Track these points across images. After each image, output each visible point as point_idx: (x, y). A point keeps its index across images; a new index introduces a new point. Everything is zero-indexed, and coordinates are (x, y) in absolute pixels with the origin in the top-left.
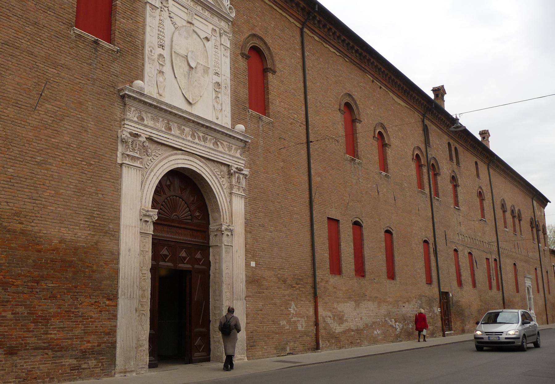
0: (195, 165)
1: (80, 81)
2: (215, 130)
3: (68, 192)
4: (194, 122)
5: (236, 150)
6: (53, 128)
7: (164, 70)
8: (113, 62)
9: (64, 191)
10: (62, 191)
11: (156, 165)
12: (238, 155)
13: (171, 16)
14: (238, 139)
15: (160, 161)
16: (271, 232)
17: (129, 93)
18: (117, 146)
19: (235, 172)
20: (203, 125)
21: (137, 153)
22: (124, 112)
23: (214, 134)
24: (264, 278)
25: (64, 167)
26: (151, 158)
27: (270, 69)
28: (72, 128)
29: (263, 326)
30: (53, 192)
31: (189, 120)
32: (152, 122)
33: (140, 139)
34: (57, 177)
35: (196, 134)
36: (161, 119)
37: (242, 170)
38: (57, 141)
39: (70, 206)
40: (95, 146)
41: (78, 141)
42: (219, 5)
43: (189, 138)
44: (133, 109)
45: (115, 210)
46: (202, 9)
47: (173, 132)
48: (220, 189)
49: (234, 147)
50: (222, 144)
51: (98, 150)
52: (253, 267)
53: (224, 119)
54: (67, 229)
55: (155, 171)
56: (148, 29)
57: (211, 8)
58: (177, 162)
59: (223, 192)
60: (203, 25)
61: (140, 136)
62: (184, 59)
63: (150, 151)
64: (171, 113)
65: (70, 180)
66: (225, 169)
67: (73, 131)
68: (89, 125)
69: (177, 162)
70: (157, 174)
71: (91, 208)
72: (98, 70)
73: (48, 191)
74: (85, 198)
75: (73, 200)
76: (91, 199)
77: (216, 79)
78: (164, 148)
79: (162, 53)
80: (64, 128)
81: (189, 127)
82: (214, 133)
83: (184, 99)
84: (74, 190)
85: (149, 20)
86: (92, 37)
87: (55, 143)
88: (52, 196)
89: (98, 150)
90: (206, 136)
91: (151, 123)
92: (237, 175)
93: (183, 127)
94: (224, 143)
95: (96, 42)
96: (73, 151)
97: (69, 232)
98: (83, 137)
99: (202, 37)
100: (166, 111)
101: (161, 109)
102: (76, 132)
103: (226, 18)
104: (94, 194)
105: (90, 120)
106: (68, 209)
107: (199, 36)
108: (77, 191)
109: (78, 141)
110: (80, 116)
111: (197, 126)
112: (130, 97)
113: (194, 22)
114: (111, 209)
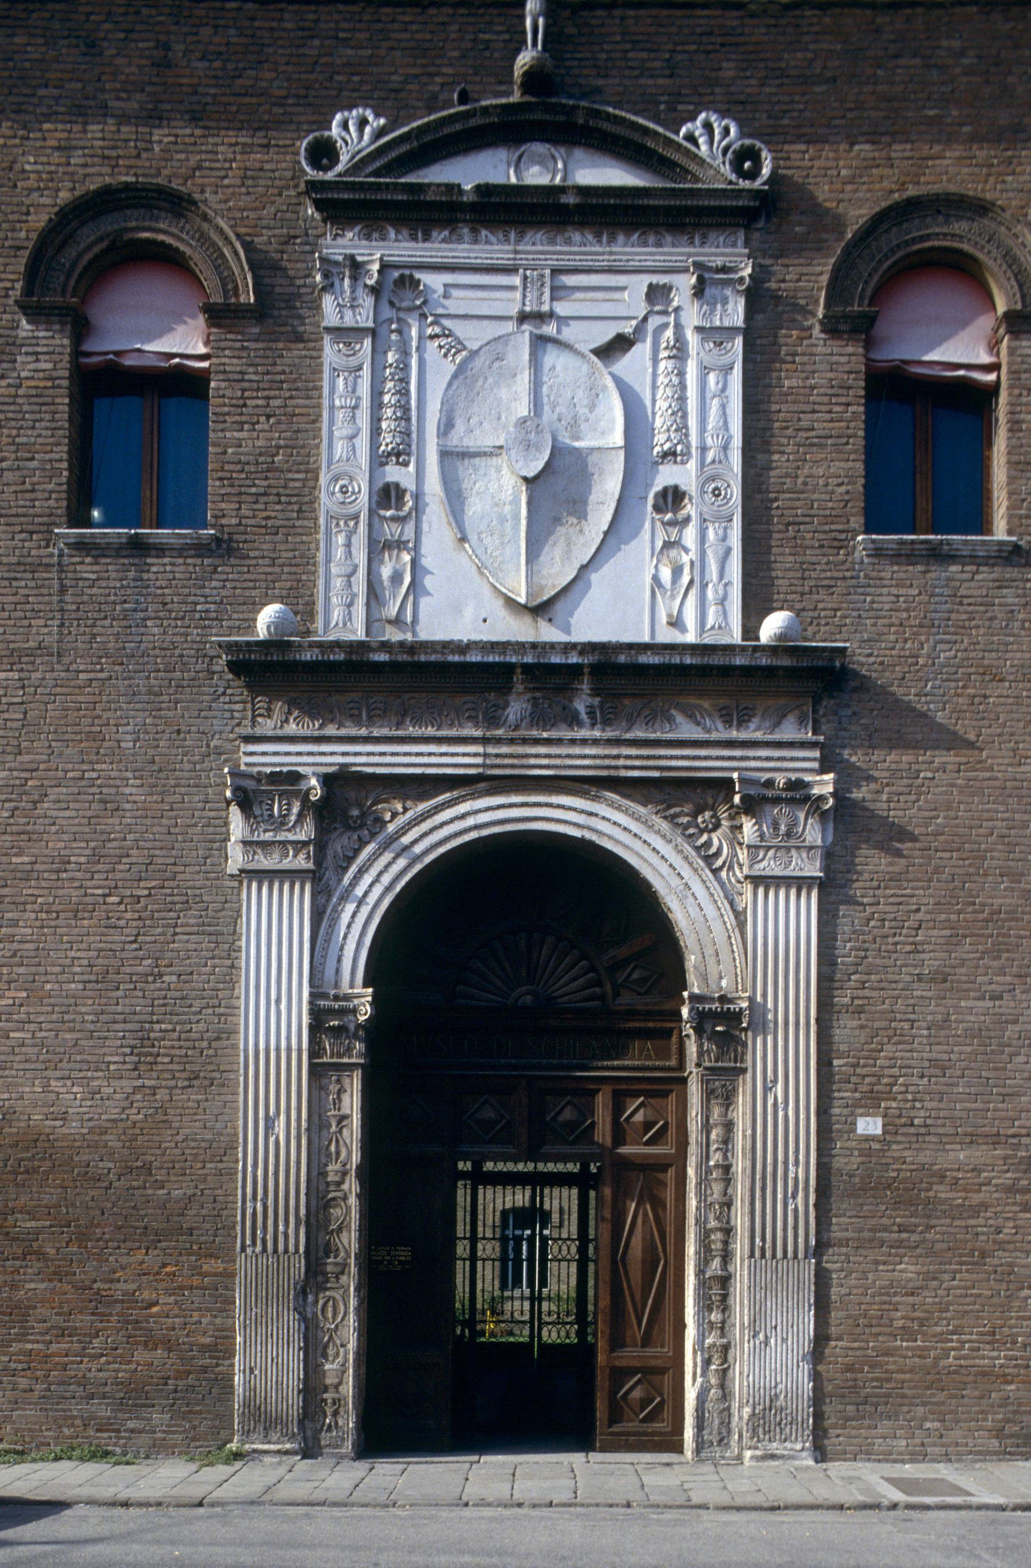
1: (92, 675)
3: (65, 986)
6: (14, 828)
9: (56, 986)
10: (48, 987)
16: (996, 997)
18: (226, 824)
25: (53, 923)
28: (73, 814)
30: (24, 994)
34: (33, 954)
38: (26, 859)
39: (74, 1021)
40: (149, 845)
41: (92, 844)
45: (222, 1010)
51: (157, 852)
52: (868, 1139)
54: (69, 1083)
58: (471, 821)
65: (73, 954)
67: (76, 821)
68: (127, 791)
69: (471, 821)
71: (137, 1018)
73: (12, 994)
74: (120, 993)
75: (84, 1005)
76: (140, 994)
80: (47, 821)
84: (86, 977)
87: (20, 867)
88: (21, 1005)
89: (157, 852)
96: (79, 875)
97: (75, 1089)
98: (109, 829)
104: (150, 979)
105: (130, 775)
106: (72, 1030)
108: (93, 978)
109: (92, 844)
110: (94, 775)
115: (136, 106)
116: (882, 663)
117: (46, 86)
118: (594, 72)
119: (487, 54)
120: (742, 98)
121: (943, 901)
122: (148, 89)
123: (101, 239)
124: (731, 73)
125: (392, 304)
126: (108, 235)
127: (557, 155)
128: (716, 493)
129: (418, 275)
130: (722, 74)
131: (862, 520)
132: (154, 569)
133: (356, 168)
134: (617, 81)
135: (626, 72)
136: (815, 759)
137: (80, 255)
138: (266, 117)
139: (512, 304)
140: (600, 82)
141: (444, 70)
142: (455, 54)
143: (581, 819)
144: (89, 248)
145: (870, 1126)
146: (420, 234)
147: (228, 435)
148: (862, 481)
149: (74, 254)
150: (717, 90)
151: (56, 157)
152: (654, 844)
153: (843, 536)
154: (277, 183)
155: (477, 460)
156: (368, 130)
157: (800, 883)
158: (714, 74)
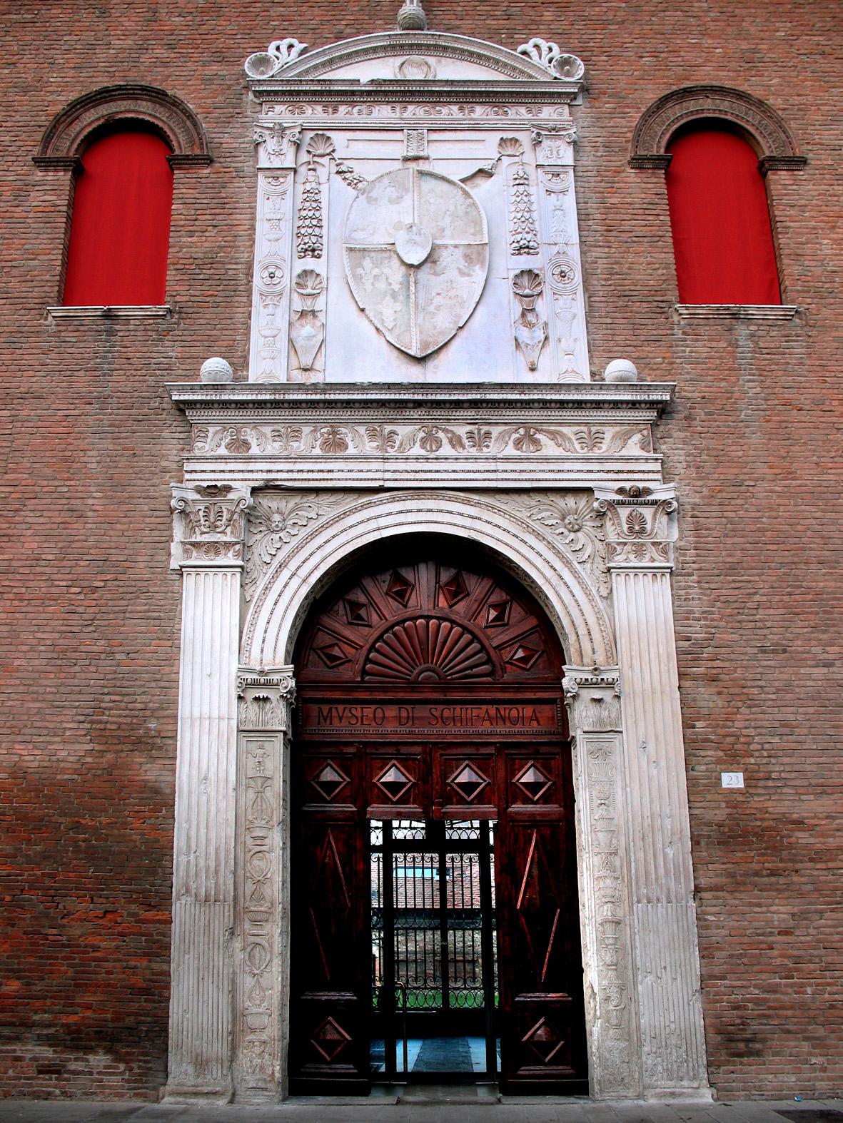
0: (448, 518)
2: (510, 404)
4: (418, 404)
5: (626, 437)
7: (320, 304)
8: (160, 340)
11: (298, 549)
12: (633, 448)
13: (343, 168)
14: (616, 405)
15: (313, 535)
17: (182, 398)
19: (612, 505)
20: (458, 404)
21: (223, 532)
22: (188, 445)
23: (511, 414)
24: (799, 822)
26: (281, 534)
27: (772, 159)
29: (802, 986)
31: (401, 404)
32: (277, 445)
33: (231, 496)
35: (441, 435)
36: (306, 430)
37: (647, 491)
42: (523, 72)
43: (417, 451)
44: (212, 429)
46: (461, 109)
47: (351, 451)
48: (558, 565)
49: (609, 432)
50: (553, 435)
52: (732, 791)
53: (566, 360)
55: (293, 565)
56: (262, 229)
57: (488, 94)
58: (373, 525)
59: (574, 573)
60: (466, 145)
61: (228, 489)
62: (387, 254)
63: (277, 517)
64: (330, 404)
66: (582, 501)
69: (373, 525)
70: (303, 572)
72: (115, 373)
77: (524, 262)
78: (325, 499)
79: (308, 268)
81: (410, 421)
82: (510, 413)
83: (395, 353)
85: (264, 208)
86: (100, 309)
90: (485, 429)
91: (273, 448)
92: (624, 512)
93: (388, 428)
94: (565, 430)
95: (108, 316)
99: (456, 179)
100: (312, 404)
101: (296, 404)
102: (55, 526)
103: (552, 95)
107: (443, 179)
111: (437, 413)
112: (191, 404)
113: (433, 151)
114: (153, 684)
115: (130, 42)
116: (703, 397)
117: (70, 35)
118: (454, 17)
119: (378, 8)
120: (560, 31)
121: (775, 585)
122: (140, 33)
123: (98, 119)
124: (551, 18)
125: (309, 152)
126: (103, 117)
127: (430, 63)
128: (563, 275)
129: (328, 134)
130: (543, 18)
131: (677, 293)
132: (121, 334)
133: (283, 70)
134: (470, 22)
135: (477, 17)
136: (658, 472)
137: (82, 129)
138: (221, 46)
139: (399, 150)
140: (458, 23)
141: (348, 17)
142: (356, 9)
143: (468, 522)
144: (89, 124)
145: (733, 780)
146: (330, 110)
147: (184, 239)
148: (675, 267)
149: (78, 129)
150: (541, 27)
151: (72, 73)
152: (530, 542)
153: (663, 305)
154: (228, 82)
155: (373, 254)
156: (293, 49)
157: (655, 572)
158: (538, 18)
